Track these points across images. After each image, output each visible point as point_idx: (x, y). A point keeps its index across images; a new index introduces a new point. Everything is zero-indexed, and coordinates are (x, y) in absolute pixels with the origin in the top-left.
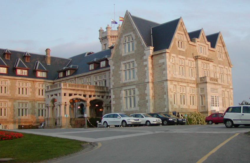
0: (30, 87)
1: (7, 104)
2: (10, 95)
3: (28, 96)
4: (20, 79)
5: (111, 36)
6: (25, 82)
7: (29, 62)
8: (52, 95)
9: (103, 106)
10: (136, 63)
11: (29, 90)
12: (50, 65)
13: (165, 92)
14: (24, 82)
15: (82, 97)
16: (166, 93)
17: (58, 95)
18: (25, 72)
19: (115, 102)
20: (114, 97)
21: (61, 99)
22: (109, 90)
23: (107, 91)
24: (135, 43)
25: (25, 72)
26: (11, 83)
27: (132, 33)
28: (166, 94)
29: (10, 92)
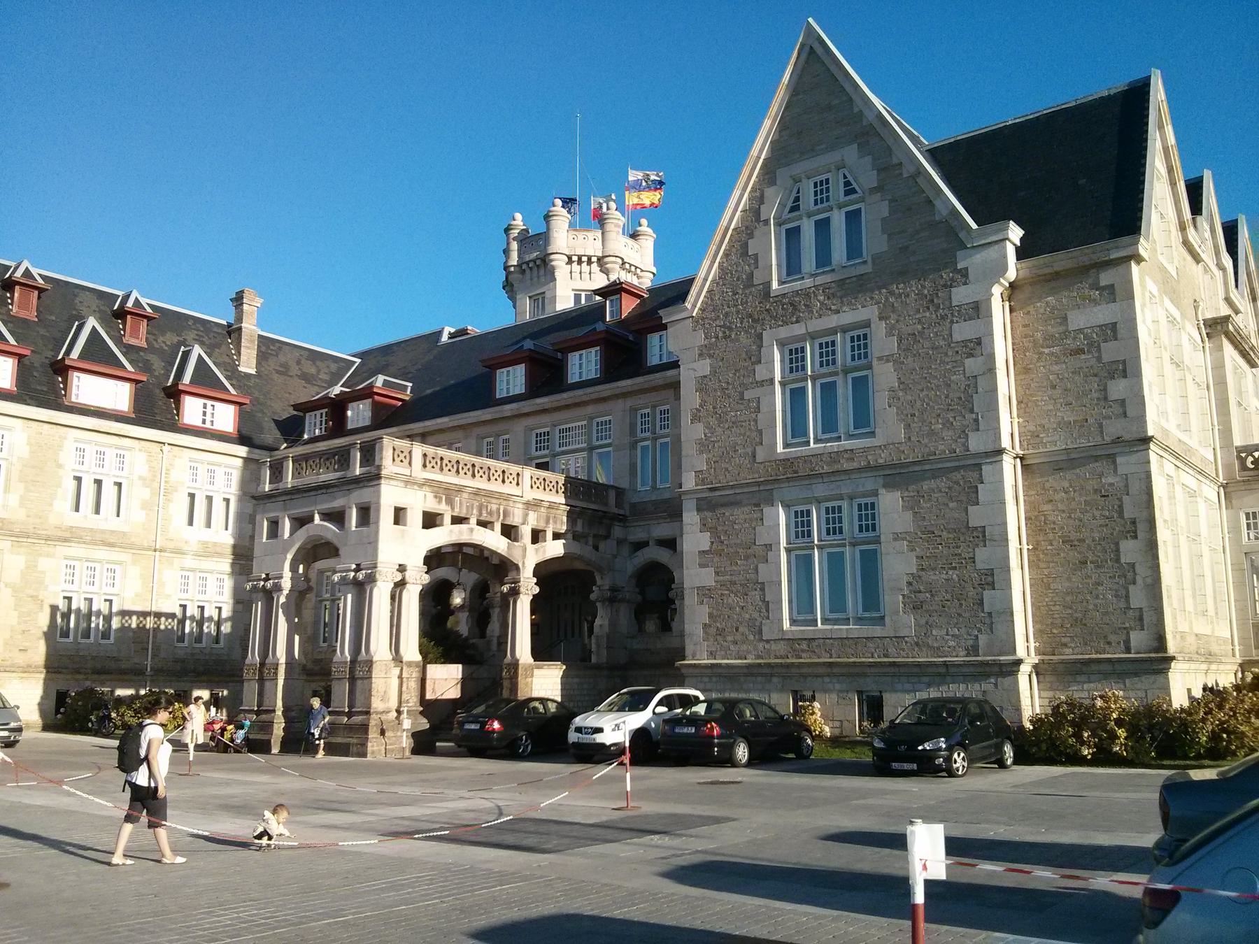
0: (141, 478)
3: (126, 529)
5: (570, 258)
7: (144, 345)
9: (593, 597)
10: (889, 334)
11: (135, 496)
12: (253, 371)
13: (1134, 522)
15: (493, 540)
16: (1142, 528)
17: (353, 517)
18: (117, 395)
19: (717, 573)
20: (707, 548)
21: (373, 543)
22: (627, 506)
23: (622, 512)
24: (875, 213)
25: (117, 395)
27: (850, 153)
28: (1141, 535)
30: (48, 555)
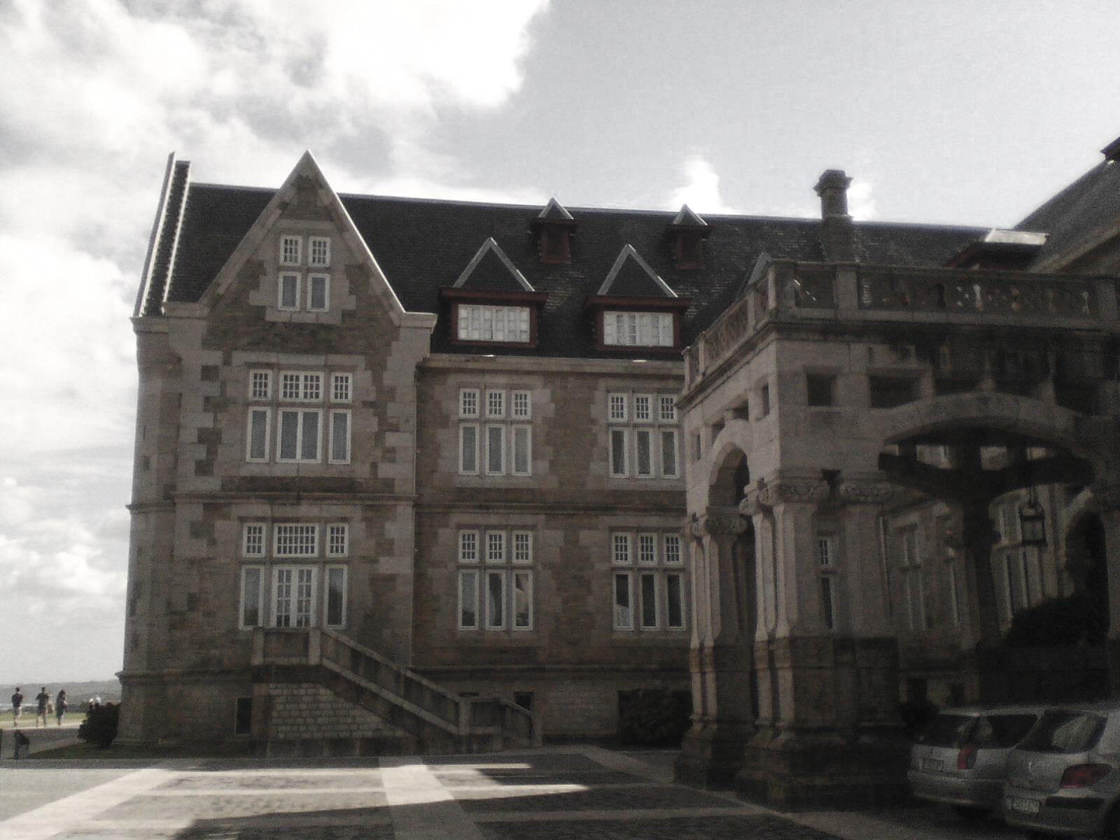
1: (535, 540)
2: (552, 483)
4: (621, 370)
6: (659, 391)
8: (719, 426)
14: (648, 391)
26: (553, 400)
29: (552, 463)
30: (590, 528)
